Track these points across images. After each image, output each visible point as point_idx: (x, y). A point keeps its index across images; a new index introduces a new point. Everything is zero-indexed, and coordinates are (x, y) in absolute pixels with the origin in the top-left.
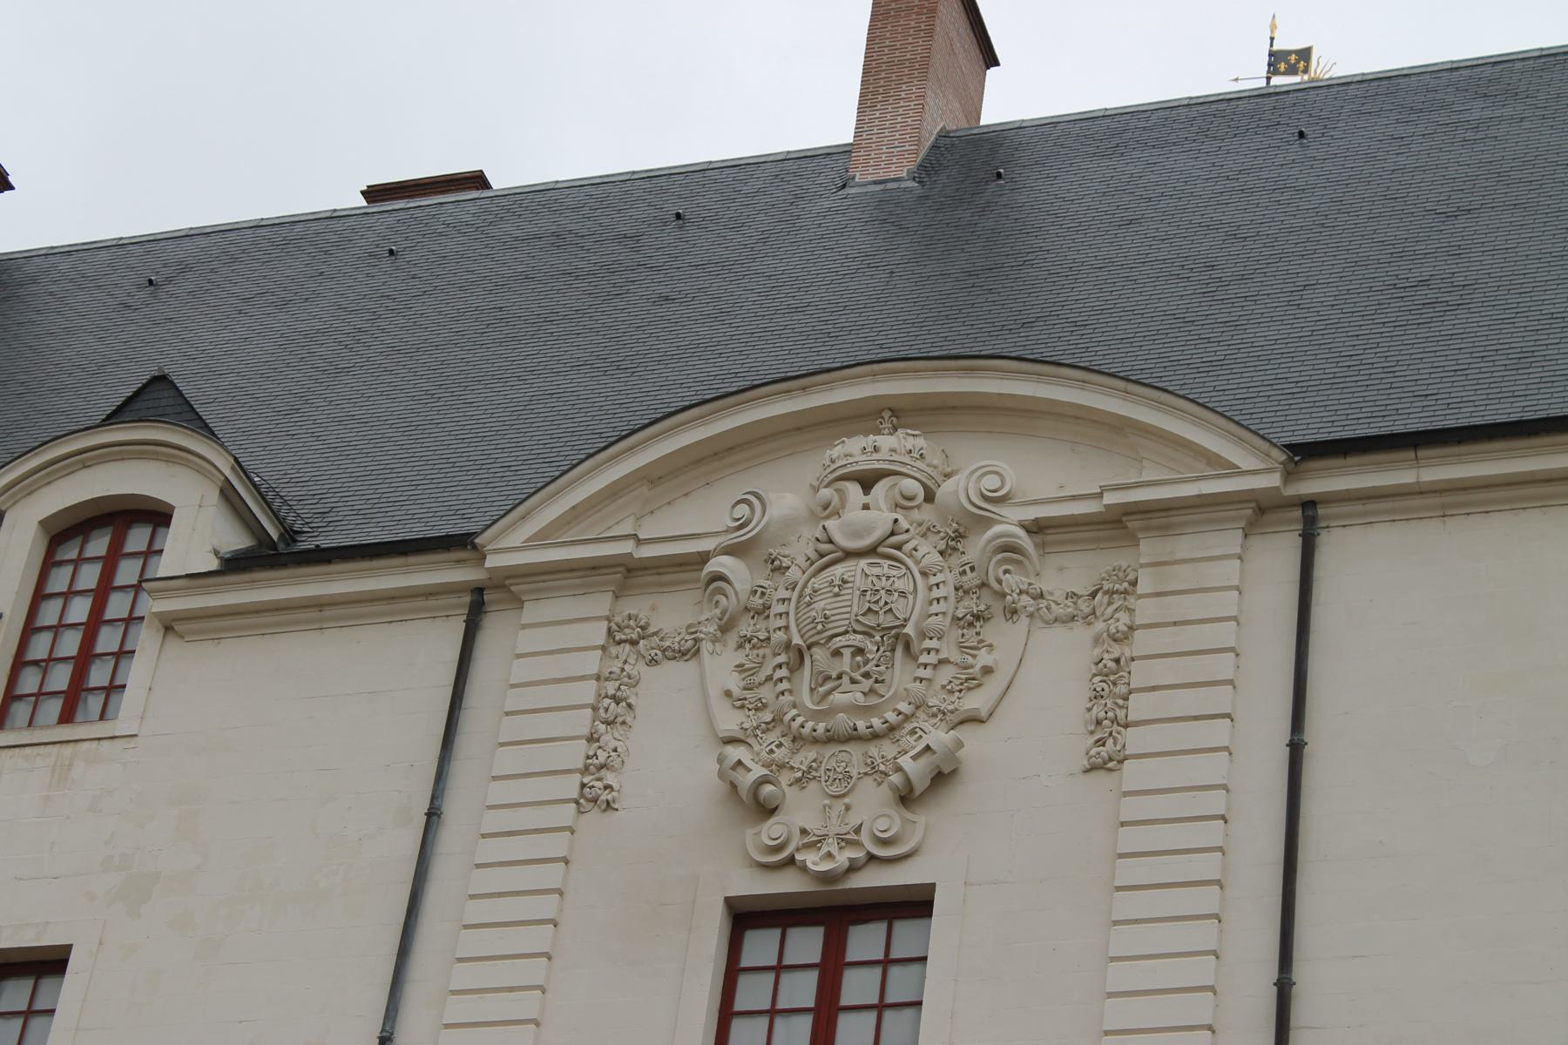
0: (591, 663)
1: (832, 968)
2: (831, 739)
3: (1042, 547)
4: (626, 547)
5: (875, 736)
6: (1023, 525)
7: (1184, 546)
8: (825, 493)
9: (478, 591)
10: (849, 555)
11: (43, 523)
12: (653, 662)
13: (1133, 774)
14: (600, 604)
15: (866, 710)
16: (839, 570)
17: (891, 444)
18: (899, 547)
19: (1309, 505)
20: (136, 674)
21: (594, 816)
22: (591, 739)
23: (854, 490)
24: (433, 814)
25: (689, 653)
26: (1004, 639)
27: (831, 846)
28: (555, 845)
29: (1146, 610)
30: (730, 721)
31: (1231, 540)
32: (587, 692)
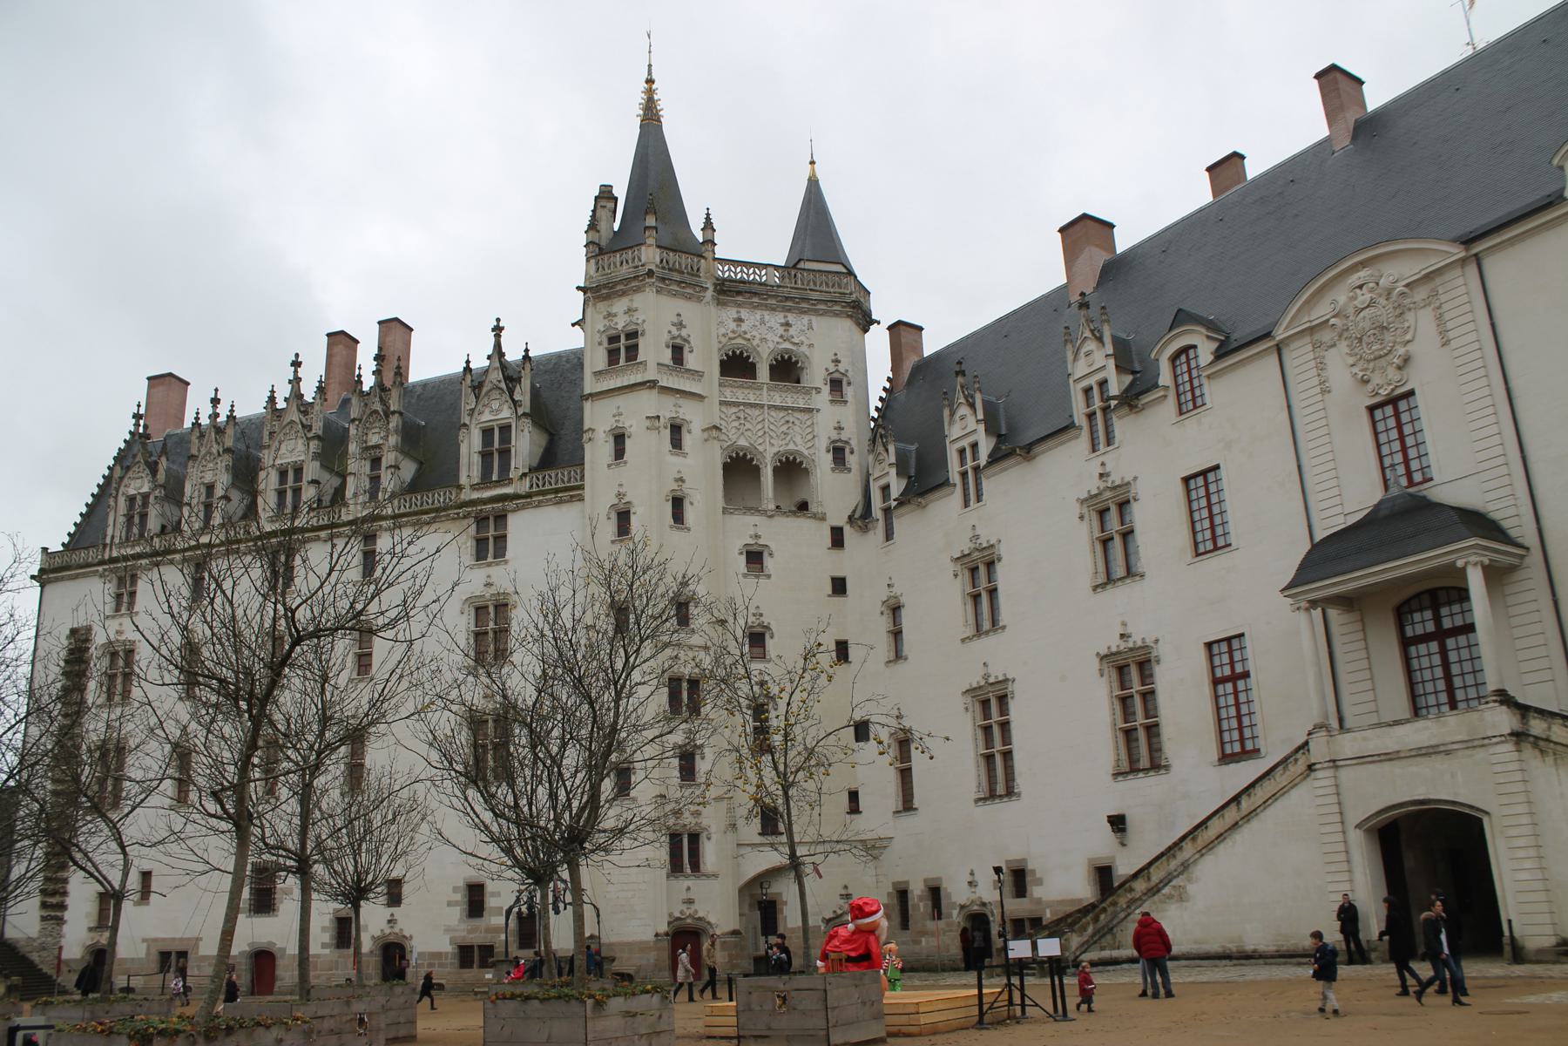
0: (1311, 356)
1: (1397, 414)
2: (1375, 359)
3: (1411, 289)
4: (1308, 325)
5: (1386, 354)
6: (1405, 286)
7: (1447, 277)
8: (1351, 294)
9: (1277, 345)
10: (1363, 309)
13: (1454, 344)
14: (1307, 339)
15: (1382, 349)
16: (1362, 314)
17: (1363, 274)
19: (1476, 255)
20: (1206, 389)
21: (1327, 395)
22: (1319, 375)
23: (1358, 291)
24: (1289, 407)
25: (1334, 345)
26: (1410, 316)
29: (1443, 298)
30: (1351, 360)
31: (1458, 272)
32: (1313, 364)
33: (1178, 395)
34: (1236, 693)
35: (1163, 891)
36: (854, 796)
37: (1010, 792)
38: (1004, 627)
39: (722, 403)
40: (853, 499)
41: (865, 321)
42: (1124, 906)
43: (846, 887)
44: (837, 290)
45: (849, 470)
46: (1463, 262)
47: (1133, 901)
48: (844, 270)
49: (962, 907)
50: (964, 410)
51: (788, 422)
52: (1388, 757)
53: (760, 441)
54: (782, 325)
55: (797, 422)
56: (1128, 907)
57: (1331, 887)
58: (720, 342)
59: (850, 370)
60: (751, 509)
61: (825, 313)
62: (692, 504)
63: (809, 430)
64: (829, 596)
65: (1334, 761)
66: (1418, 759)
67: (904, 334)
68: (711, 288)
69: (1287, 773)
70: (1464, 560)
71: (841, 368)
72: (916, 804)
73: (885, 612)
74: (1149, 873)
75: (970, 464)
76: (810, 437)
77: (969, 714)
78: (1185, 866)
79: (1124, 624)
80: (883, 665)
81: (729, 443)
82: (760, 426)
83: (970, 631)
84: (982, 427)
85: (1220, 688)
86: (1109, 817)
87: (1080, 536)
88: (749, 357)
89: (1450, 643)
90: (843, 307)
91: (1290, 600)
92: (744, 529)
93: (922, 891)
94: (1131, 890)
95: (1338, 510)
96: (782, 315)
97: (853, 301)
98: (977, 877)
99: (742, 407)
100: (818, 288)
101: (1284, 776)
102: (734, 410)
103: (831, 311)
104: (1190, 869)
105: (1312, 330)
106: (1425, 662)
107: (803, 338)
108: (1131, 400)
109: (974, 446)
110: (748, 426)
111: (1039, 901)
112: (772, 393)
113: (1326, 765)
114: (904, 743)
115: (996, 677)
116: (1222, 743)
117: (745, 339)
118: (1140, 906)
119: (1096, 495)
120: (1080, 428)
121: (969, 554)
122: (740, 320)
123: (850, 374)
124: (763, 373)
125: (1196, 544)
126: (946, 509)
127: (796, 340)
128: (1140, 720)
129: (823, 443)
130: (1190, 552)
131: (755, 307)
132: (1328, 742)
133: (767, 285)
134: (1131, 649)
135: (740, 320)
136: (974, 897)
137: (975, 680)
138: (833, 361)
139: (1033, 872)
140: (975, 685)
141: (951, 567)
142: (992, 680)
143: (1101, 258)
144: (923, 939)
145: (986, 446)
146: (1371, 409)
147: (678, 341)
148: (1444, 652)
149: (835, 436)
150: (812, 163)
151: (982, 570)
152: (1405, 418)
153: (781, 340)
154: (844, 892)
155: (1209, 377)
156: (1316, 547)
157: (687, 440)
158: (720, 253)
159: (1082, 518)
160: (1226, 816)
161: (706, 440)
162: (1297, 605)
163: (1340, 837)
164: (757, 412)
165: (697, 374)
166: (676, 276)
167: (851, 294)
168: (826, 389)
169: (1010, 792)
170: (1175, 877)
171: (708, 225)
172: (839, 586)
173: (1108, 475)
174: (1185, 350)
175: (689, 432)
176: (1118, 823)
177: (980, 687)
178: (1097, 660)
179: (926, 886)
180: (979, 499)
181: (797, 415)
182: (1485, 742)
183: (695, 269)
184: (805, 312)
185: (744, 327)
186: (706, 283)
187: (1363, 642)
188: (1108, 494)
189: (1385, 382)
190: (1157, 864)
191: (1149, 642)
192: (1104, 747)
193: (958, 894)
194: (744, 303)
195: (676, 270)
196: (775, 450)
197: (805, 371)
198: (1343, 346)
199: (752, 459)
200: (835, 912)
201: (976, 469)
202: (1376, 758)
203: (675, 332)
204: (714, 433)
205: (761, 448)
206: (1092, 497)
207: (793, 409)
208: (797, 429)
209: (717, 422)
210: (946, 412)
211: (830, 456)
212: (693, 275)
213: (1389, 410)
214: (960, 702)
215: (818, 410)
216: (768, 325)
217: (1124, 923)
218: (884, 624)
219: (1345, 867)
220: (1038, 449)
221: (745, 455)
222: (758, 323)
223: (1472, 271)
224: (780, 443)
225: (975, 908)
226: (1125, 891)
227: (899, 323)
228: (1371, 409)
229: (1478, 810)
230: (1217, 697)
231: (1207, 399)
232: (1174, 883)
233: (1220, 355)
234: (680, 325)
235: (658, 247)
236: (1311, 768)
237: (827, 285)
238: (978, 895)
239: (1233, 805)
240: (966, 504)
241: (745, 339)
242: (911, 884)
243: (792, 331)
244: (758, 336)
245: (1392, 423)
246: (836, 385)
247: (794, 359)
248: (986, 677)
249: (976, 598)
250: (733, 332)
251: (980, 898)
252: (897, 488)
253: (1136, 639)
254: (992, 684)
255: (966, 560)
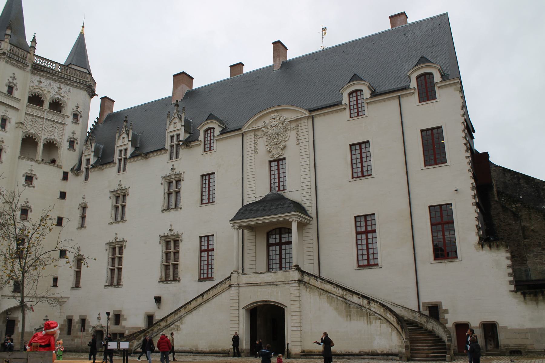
0: (253, 139)
1: (278, 165)
2: (275, 145)
3: (290, 123)
4: (254, 128)
5: (278, 144)
6: (288, 121)
7: (302, 121)
8: (271, 121)
9: (243, 133)
10: (273, 127)
11: (204, 131)
12: (259, 138)
14: (253, 133)
15: (277, 142)
16: (273, 128)
17: (276, 114)
18: (278, 125)
19: (312, 116)
20: (215, 144)
22: (255, 147)
23: (273, 120)
24: (243, 156)
25: (262, 137)
26: (288, 132)
27: (276, 155)
28: (253, 158)
29: (300, 128)
30: (266, 144)
31: (306, 120)
32: (253, 142)
33: (205, 145)
34: (208, 256)
35: (171, 327)
36: (56, 280)
37: (119, 284)
38: (126, 221)
39: (26, 114)
40: (74, 162)
41: (92, 94)
42: (156, 331)
43: (47, 316)
44: (83, 79)
45: (75, 150)
46: (308, 117)
47: (160, 329)
48: (88, 72)
49: (94, 327)
50: (125, 135)
51: (53, 127)
52: (257, 284)
53: (40, 132)
54: (58, 88)
55: (57, 128)
56: (158, 332)
57: (231, 329)
58: (30, 89)
59: (82, 111)
60: (31, 159)
61: (76, 87)
62: (5, 152)
63: (61, 132)
64: (58, 199)
65: (239, 284)
66: (267, 286)
67: (106, 102)
68: (30, 66)
69: (222, 287)
70: (292, 219)
71: (79, 110)
72: (81, 285)
73: (80, 208)
74: (167, 319)
75: (123, 156)
76: (61, 134)
77: (107, 253)
78: (181, 318)
79: (171, 226)
80: (76, 229)
81: (27, 130)
82: (41, 126)
83: (112, 220)
84: (130, 143)
85: (203, 253)
86: (155, 297)
87: (160, 190)
88: (41, 98)
89: (283, 247)
90: (84, 86)
91: (232, 225)
92: (26, 166)
93: (78, 320)
94: (160, 325)
95: (253, 195)
96: (59, 84)
97: (89, 85)
98: (101, 316)
99: (34, 117)
100: (75, 76)
101: (221, 288)
102: (31, 117)
103: (79, 87)
104: (182, 319)
105: (255, 130)
106: (274, 253)
107: (65, 95)
108: (188, 143)
109: (126, 150)
110: (36, 125)
111: (124, 327)
112: (48, 114)
113: (235, 285)
114: (79, 261)
115: (120, 239)
116: (200, 274)
117: (41, 90)
118: (162, 331)
119: (169, 176)
120: (167, 150)
121: (117, 191)
122: (40, 82)
123: (82, 113)
124: (46, 105)
125: (202, 200)
126: (111, 171)
127: (62, 95)
128: (172, 262)
129: (66, 138)
130: (199, 202)
131: (48, 78)
132: (237, 277)
133: (55, 71)
134: (172, 235)
135: (40, 82)
136: (99, 324)
137: (111, 239)
138: (76, 107)
139: (123, 315)
140: (111, 241)
141: (109, 195)
142: (118, 240)
143: (186, 89)
144: (76, 339)
145: (130, 151)
146: (270, 162)
147: (12, 84)
148: (281, 250)
149: (71, 136)
150: (83, 27)
151: (121, 197)
152: (281, 167)
153: (56, 94)
154: (45, 318)
155: (217, 140)
156: (244, 207)
157: (8, 126)
158: (37, 53)
159: (162, 184)
160: (198, 301)
161: (16, 127)
162: (234, 227)
163: (237, 311)
164: (41, 120)
165: (18, 100)
166: (15, 58)
167: (88, 82)
168: (71, 117)
169: (119, 284)
170: (176, 322)
171: (34, 40)
172: (63, 195)
173: (174, 169)
174: (210, 129)
175: (10, 123)
176: (158, 300)
177: (113, 243)
178: (159, 238)
179: (80, 318)
180: (124, 170)
181: (58, 125)
182: (289, 282)
183: (25, 57)
184: (68, 85)
185: (42, 85)
186: (28, 64)
187: (255, 243)
188: (173, 176)
189: (276, 153)
190: (170, 316)
191: (179, 233)
192: (157, 271)
193: (93, 322)
194: (43, 75)
195: (16, 55)
196: (46, 137)
197: (64, 108)
198: (265, 138)
199: (35, 139)
200: (40, 326)
201: (125, 159)
202: (253, 285)
203: (11, 80)
204: (21, 125)
205: (40, 135)
206: (167, 176)
207: (56, 122)
208: (56, 130)
209: (23, 121)
210: (117, 135)
211: (68, 144)
212: (23, 59)
213: (276, 163)
214: (104, 247)
215: (66, 125)
216: (52, 86)
217: (155, 337)
218: (79, 213)
219: (237, 322)
220: (150, 155)
221: (32, 137)
222: (48, 85)
223: (310, 121)
224: (48, 134)
225: (99, 328)
226: (157, 325)
227: (106, 97)
228: (270, 162)
229: (284, 305)
230: (201, 257)
231: (215, 148)
232: (175, 324)
233: (222, 133)
234: (14, 78)
235: (10, 43)
236: (230, 286)
237: (79, 76)
238: (100, 323)
239: (201, 297)
240: (119, 171)
241: (41, 90)
242: (74, 317)
243: (62, 91)
244: (47, 90)
245: (276, 168)
246: (76, 116)
247: (60, 102)
248: (116, 238)
249: (117, 208)
250: (37, 86)
251: (101, 324)
252: (93, 160)
253: (175, 232)
254: (118, 242)
255: (115, 193)
